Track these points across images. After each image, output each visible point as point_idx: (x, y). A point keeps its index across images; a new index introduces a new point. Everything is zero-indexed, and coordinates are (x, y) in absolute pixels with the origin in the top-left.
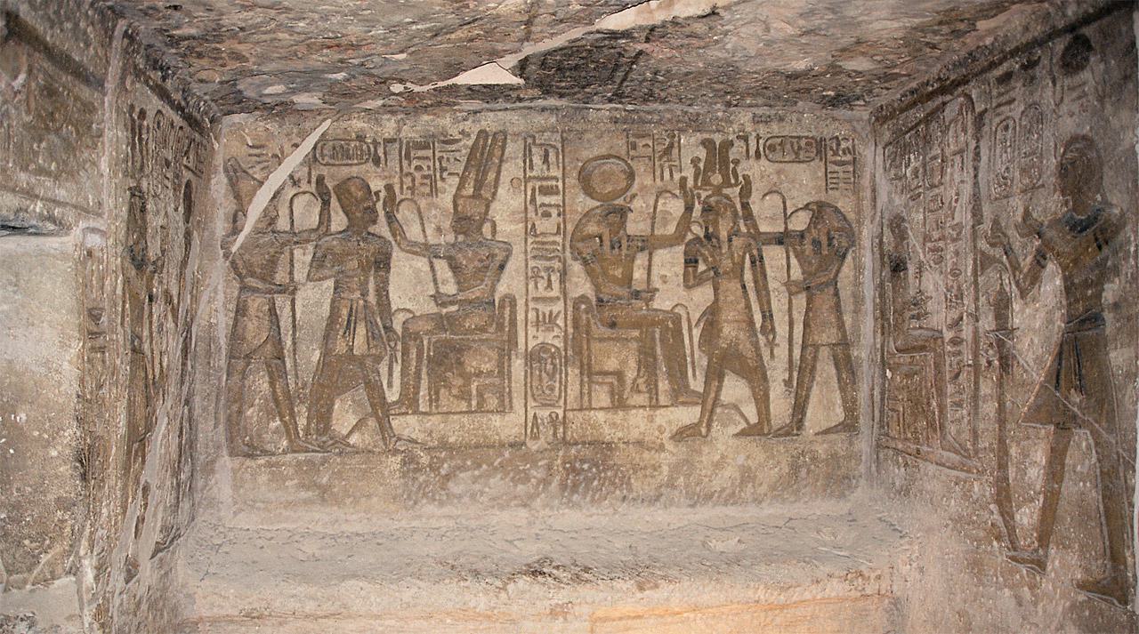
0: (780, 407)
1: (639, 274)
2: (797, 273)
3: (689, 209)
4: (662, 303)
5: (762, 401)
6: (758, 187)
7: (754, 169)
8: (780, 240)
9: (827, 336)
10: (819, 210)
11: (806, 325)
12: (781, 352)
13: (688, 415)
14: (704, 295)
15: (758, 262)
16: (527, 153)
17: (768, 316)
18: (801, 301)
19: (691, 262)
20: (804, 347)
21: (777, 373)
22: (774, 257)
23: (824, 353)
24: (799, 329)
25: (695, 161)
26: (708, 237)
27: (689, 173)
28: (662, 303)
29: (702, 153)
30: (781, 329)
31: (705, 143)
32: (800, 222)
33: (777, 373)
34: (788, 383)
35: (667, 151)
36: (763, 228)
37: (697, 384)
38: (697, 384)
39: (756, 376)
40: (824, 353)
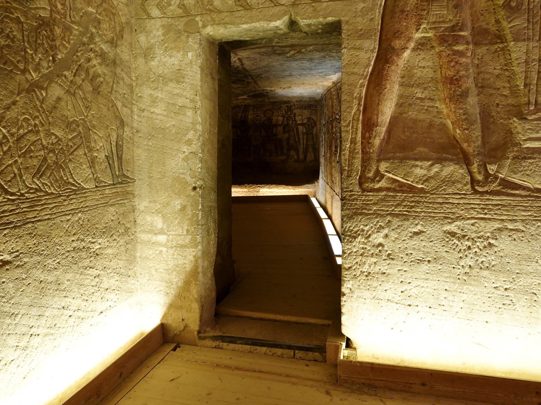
0: (301, 156)
1: (274, 131)
2: (304, 131)
3: (284, 119)
4: (279, 137)
5: (298, 155)
6: (297, 114)
7: (296, 111)
8: (301, 124)
9: (310, 143)
10: (309, 119)
11: (307, 141)
12: (302, 146)
13: (284, 158)
14: (286, 135)
15: (297, 129)
16: (254, 109)
17: (299, 139)
18: (305, 136)
19: (284, 128)
20: (306, 145)
21: (301, 150)
22: (300, 128)
23: (310, 146)
24: (305, 141)
25: (285, 110)
26: (288, 124)
27: (284, 112)
28: (279, 137)
29: (286, 108)
30: (302, 141)
31: (287, 106)
32: (305, 121)
33: (301, 150)
34: (303, 152)
35: (280, 108)
36: (298, 122)
37: (285, 152)
38: (285, 152)
39: (297, 151)
40: (310, 146)
